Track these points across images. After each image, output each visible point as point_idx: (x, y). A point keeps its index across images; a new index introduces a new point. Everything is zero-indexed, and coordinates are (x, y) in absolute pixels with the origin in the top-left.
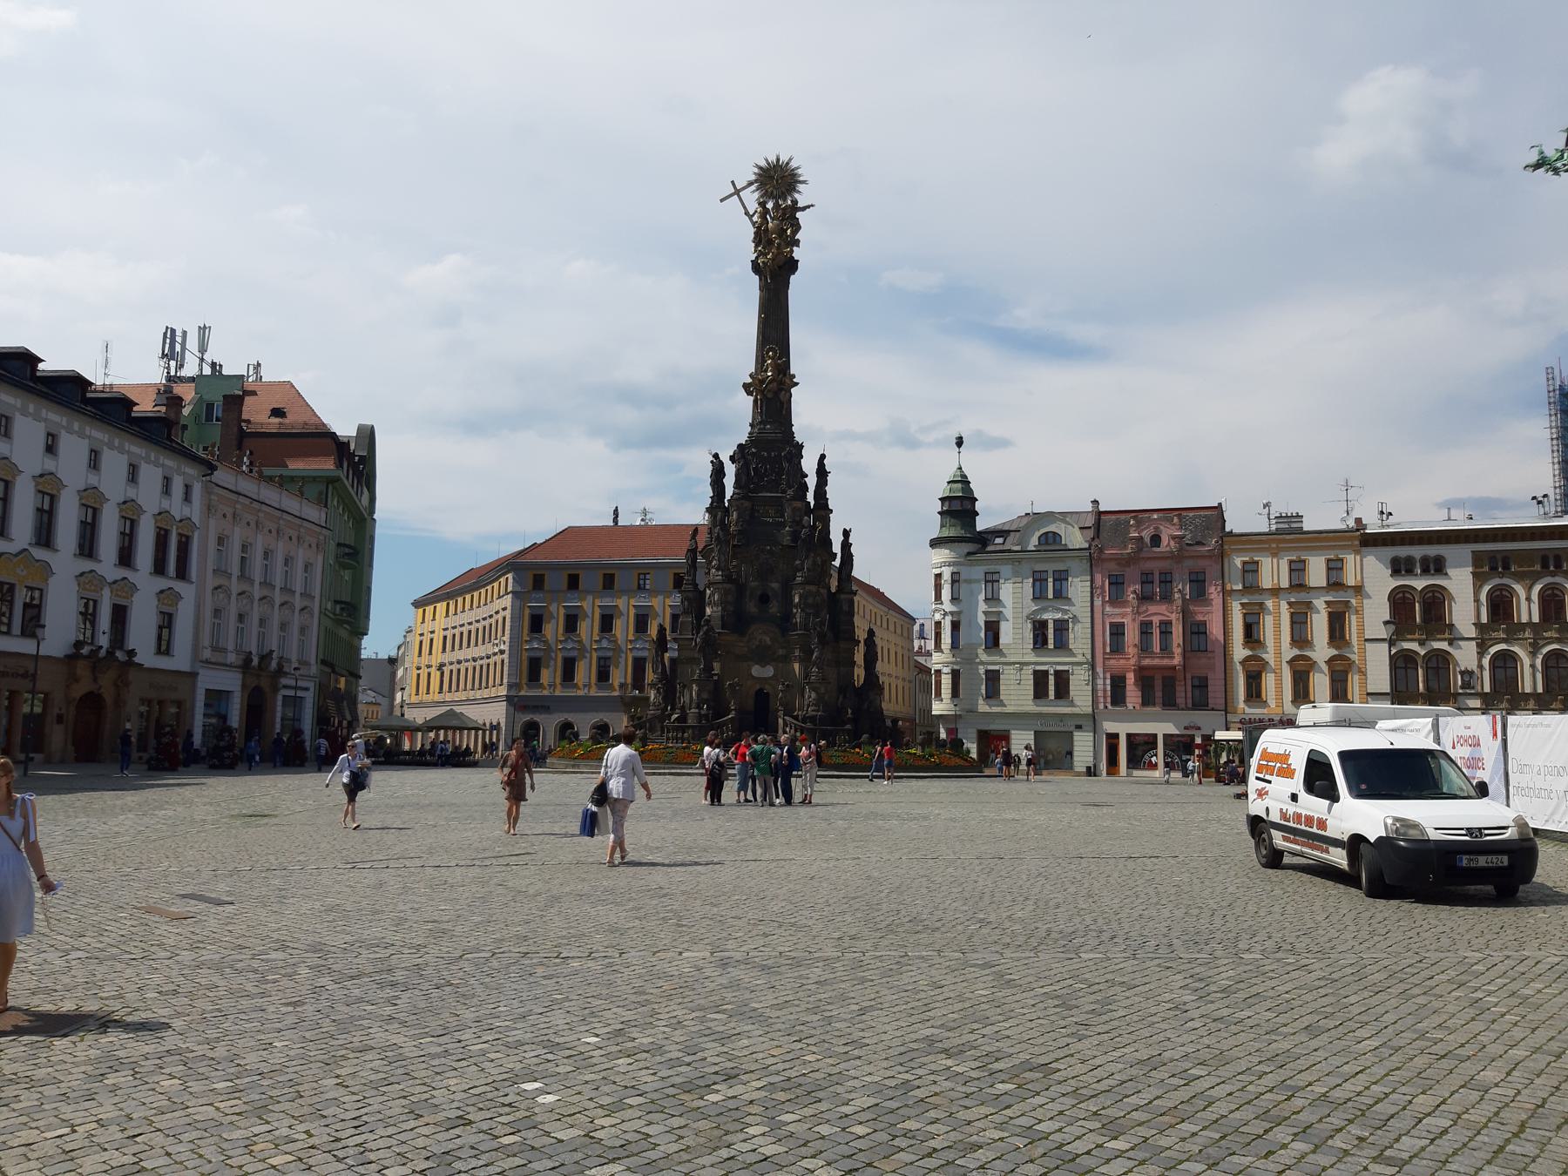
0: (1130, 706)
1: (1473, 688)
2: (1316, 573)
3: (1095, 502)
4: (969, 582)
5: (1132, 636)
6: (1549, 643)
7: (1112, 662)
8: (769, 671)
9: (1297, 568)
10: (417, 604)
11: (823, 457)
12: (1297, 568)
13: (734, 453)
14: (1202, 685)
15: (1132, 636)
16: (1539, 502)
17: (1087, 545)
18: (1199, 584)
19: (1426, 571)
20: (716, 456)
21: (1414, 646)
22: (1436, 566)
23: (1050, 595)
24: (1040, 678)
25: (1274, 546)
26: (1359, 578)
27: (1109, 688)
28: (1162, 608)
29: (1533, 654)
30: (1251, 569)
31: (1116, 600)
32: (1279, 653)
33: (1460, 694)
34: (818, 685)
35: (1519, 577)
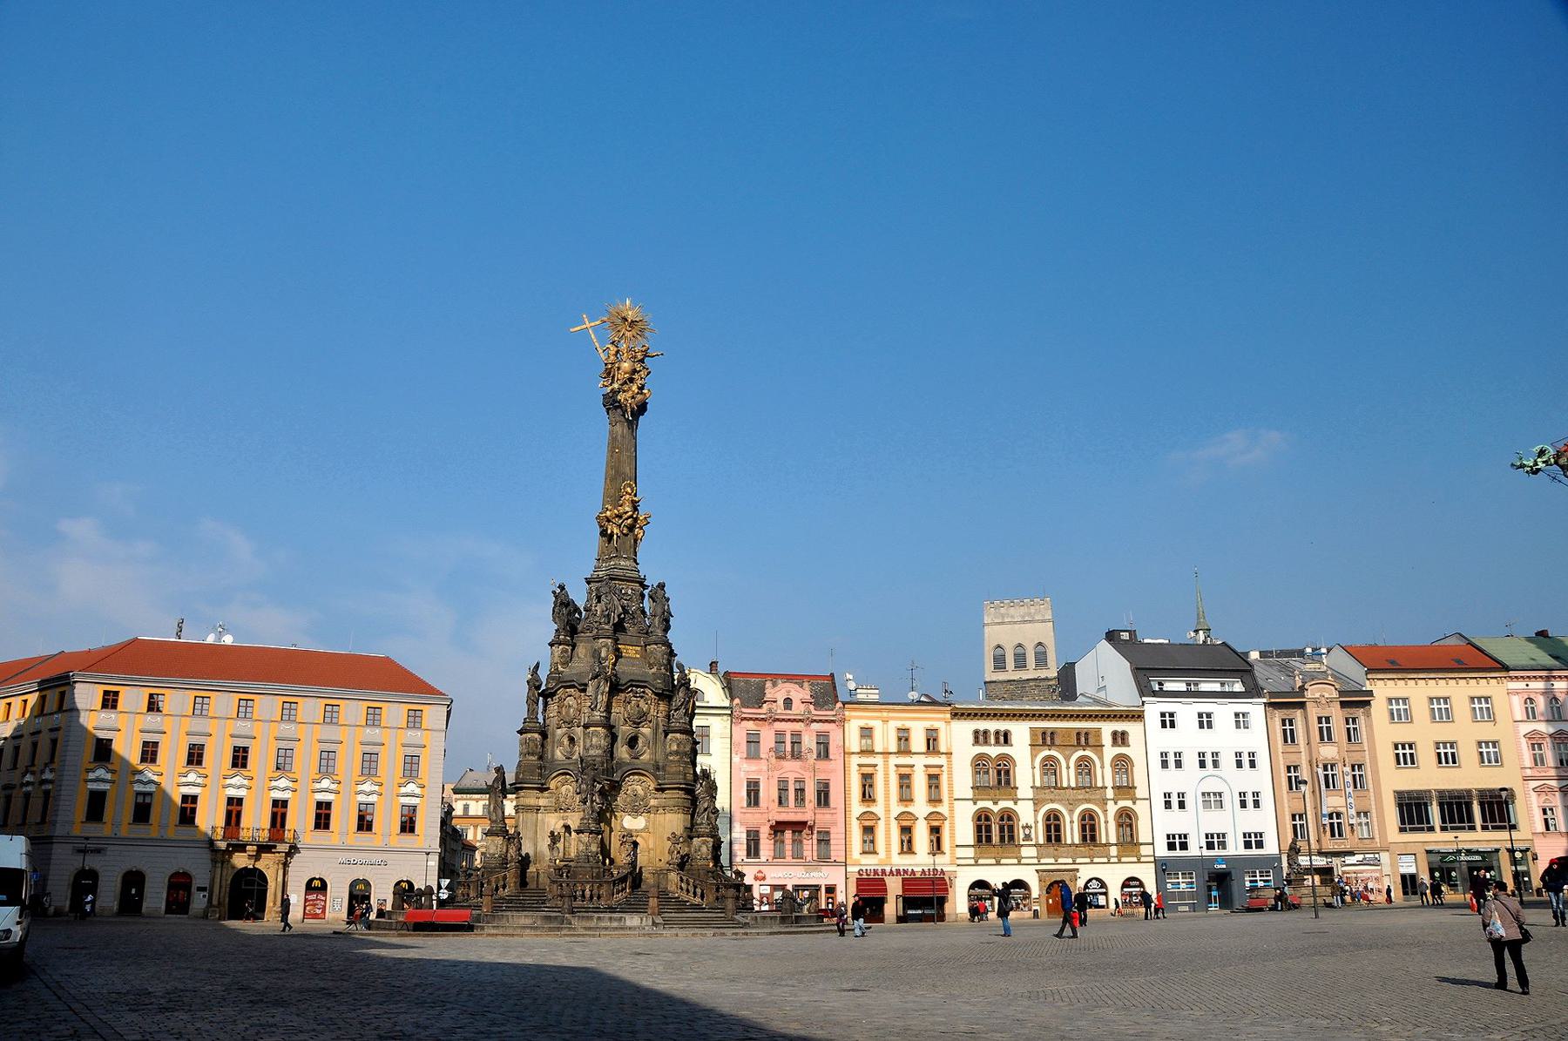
0: (763, 859)
2: (918, 742)
9: (904, 737)
12: (904, 737)
14: (824, 840)
15: (768, 793)
17: (727, 703)
19: (997, 742)
20: (562, 588)
21: (989, 804)
22: (1005, 738)
25: (885, 714)
28: (796, 764)
29: (1071, 812)
30: (867, 732)
32: (888, 811)
33: (1022, 846)
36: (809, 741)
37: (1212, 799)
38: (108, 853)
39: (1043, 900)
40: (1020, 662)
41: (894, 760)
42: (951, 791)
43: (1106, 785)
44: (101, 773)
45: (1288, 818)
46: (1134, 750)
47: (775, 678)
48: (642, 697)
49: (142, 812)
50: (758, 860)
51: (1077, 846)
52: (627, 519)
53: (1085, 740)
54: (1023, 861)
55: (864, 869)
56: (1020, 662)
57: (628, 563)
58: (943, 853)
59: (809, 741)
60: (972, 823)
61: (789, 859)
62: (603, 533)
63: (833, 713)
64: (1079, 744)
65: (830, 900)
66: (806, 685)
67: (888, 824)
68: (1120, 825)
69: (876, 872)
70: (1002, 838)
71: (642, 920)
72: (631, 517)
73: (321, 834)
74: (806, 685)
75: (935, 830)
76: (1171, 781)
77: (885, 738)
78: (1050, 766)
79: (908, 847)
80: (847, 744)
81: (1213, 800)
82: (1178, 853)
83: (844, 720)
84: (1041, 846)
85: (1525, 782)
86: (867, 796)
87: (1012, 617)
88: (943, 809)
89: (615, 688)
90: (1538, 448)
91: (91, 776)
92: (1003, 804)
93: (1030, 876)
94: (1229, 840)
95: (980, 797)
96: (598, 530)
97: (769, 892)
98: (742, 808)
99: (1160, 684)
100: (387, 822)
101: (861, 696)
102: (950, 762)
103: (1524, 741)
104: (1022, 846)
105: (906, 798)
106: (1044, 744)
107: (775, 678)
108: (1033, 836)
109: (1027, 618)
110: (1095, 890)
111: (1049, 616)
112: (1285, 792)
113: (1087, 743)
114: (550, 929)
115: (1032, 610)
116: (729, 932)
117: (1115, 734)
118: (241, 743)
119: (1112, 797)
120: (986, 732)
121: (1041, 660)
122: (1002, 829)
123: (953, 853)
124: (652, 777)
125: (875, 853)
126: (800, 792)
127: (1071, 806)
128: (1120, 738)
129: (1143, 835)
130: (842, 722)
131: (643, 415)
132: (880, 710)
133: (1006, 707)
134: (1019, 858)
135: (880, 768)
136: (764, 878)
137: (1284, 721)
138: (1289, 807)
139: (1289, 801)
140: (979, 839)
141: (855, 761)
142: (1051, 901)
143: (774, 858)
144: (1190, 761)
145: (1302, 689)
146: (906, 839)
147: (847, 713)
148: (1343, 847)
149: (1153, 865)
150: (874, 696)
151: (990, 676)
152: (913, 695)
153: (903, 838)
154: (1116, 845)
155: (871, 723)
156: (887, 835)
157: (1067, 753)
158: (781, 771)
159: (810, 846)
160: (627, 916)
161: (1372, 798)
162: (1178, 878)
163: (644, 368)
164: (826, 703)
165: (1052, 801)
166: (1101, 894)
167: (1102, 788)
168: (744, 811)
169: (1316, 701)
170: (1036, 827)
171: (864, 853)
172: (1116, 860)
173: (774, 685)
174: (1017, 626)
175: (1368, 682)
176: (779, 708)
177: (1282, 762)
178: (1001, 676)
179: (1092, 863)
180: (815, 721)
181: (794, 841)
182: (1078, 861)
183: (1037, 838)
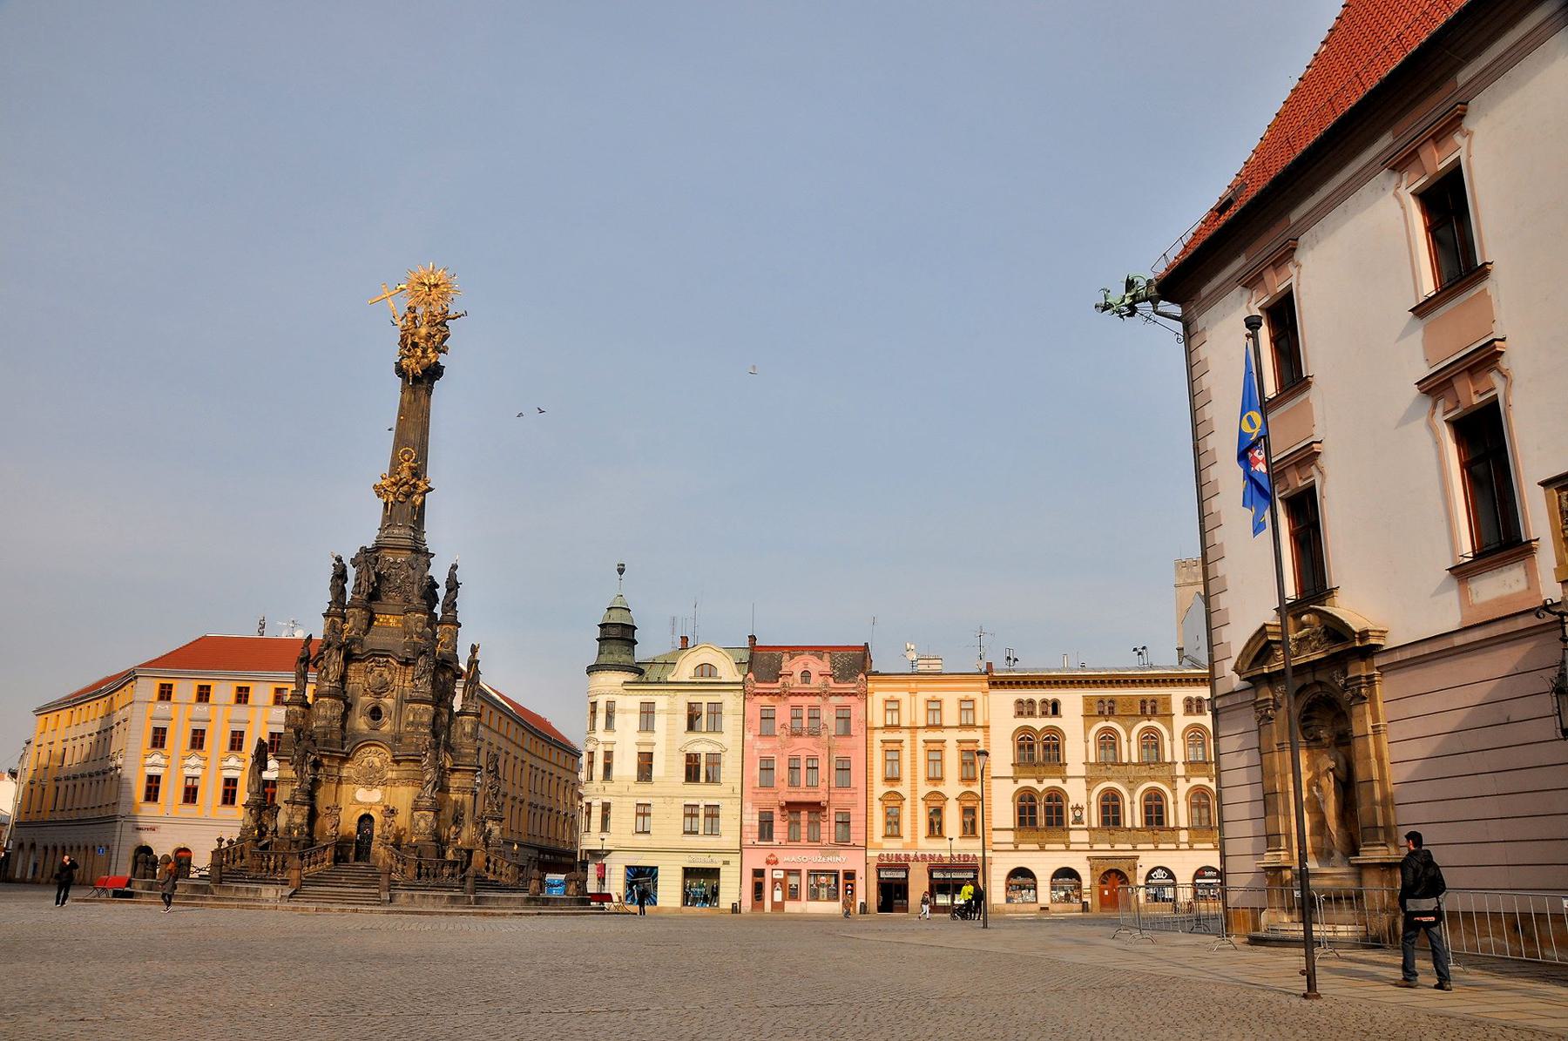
0: (776, 842)
1: (1083, 823)
2: (951, 715)
3: (753, 638)
4: (624, 712)
5: (781, 770)
6: (1146, 782)
7: (761, 796)
8: (375, 795)
9: (935, 706)
10: (41, 711)
11: (455, 567)
12: (935, 706)
13: (356, 557)
15: (781, 770)
16: (1140, 654)
17: (740, 678)
18: (844, 719)
19: (1044, 714)
20: (339, 559)
21: (1032, 783)
22: (1055, 708)
23: (704, 729)
24: (691, 812)
25: (913, 685)
26: (986, 718)
27: (757, 823)
29: (1132, 791)
30: (892, 705)
31: (765, 734)
32: (914, 791)
33: (1071, 829)
34: (426, 812)
36: (828, 716)
38: (161, 831)
39: (1096, 891)
41: (922, 735)
44: (157, 758)
47: (795, 651)
48: (385, 666)
49: (190, 795)
50: (770, 843)
51: (1138, 830)
52: (401, 486)
53: (1152, 708)
55: (885, 853)
57: (402, 531)
59: (828, 716)
61: (804, 842)
63: (854, 685)
64: (1143, 713)
65: (849, 887)
66: (826, 656)
67: (914, 805)
68: (1192, 806)
69: (898, 857)
70: (1049, 823)
71: (277, 892)
73: (189, 808)
74: (826, 656)
75: (968, 812)
78: (1108, 741)
79: (935, 828)
84: (1094, 829)
89: (349, 658)
91: (149, 761)
92: (1048, 783)
97: (782, 877)
98: (755, 788)
100: (211, 792)
102: (987, 738)
104: (1071, 829)
106: (1101, 713)
108: (1085, 818)
110: (1161, 881)
113: (1154, 712)
116: (336, 907)
117: (1189, 700)
118: (237, 728)
119: (1183, 774)
120: (1031, 702)
122: (1048, 810)
124: (388, 749)
125: (899, 836)
127: (1132, 784)
130: (865, 695)
135: (907, 744)
136: (776, 862)
140: (1022, 821)
142: (1106, 893)
146: (968, 820)
153: (966, 820)
155: (897, 695)
157: (1129, 723)
158: (790, 750)
160: (263, 887)
165: (1109, 779)
166: (1168, 885)
167: (1170, 763)
168: (758, 791)
170: (1089, 808)
171: (886, 836)
172: (1187, 846)
173: (791, 658)
179: (1156, 849)
180: (833, 694)
181: (810, 822)
183: (1089, 821)
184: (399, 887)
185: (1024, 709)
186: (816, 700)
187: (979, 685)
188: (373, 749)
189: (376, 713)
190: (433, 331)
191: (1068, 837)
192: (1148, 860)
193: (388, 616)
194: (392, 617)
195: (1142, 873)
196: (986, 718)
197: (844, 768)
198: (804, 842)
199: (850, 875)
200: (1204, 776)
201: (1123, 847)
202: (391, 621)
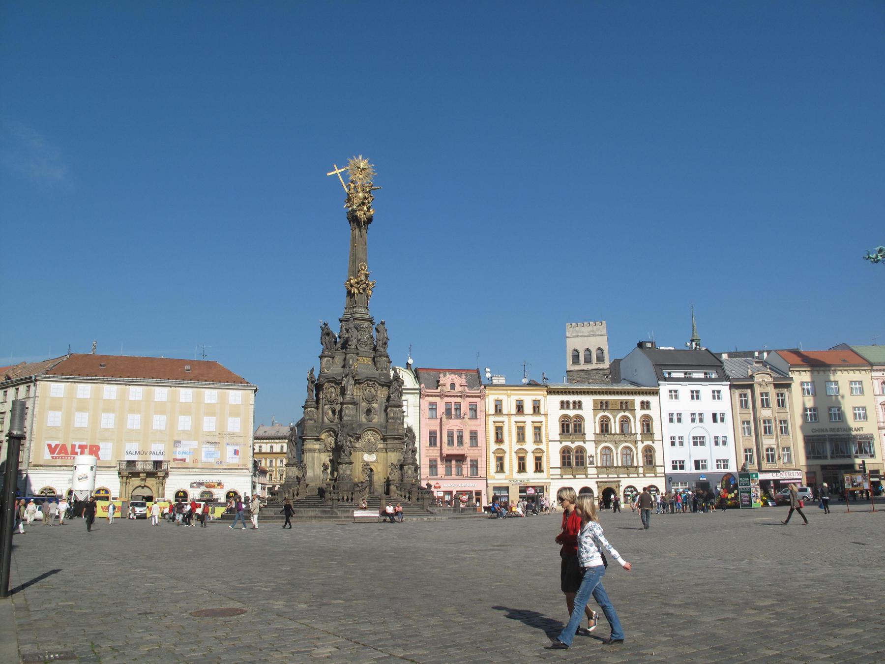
0: (439, 476)
1: (594, 464)
2: (528, 408)
14: (474, 465)
17: (417, 386)
18: (474, 409)
21: (569, 444)
22: (578, 405)
25: (509, 392)
26: (546, 410)
29: (617, 448)
32: (511, 448)
35: (612, 410)
37: (698, 440)
40: (588, 359)
42: (547, 436)
43: (637, 432)
45: (742, 451)
46: (653, 412)
48: (372, 387)
52: (362, 284)
53: (626, 406)
54: (589, 476)
56: (588, 359)
58: (542, 471)
60: (559, 455)
61: (454, 476)
62: (350, 294)
63: (479, 391)
66: (463, 376)
67: (511, 455)
70: (577, 464)
72: (365, 283)
74: (463, 376)
75: (538, 460)
76: (675, 430)
77: (509, 406)
79: (522, 468)
80: (487, 410)
81: (698, 441)
82: (678, 471)
83: (484, 396)
84: (599, 467)
85: (880, 430)
86: (499, 440)
87: (583, 332)
88: (543, 446)
90: (878, 248)
92: (577, 444)
93: (592, 484)
94: (709, 464)
95: (564, 440)
96: (346, 291)
97: (442, 495)
99: (669, 373)
101: (495, 381)
103: (880, 406)
105: (521, 438)
106: (601, 409)
107: (445, 371)
109: (592, 333)
111: (605, 332)
112: (741, 436)
114: (326, 518)
115: (595, 328)
117: (642, 403)
119: (640, 439)
120: (568, 402)
121: (601, 358)
122: (577, 458)
123: (548, 472)
126: (460, 438)
127: (616, 443)
128: (645, 405)
129: (658, 461)
131: (370, 224)
132: (506, 390)
133: (579, 387)
134: (586, 475)
135: (506, 423)
136: (440, 487)
137: (741, 396)
138: (743, 445)
139: (743, 441)
141: (491, 419)
143: (446, 475)
144: (686, 418)
145: (752, 377)
147: (487, 392)
148: (774, 468)
149: (664, 478)
150: (502, 381)
151: (570, 366)
152: (525, 381)
154: (642, 467)
155: (500, 397)
156: (510, 463)
157: (615, 414)
158: (448, 426)
159: (466, 468)
161: (792, 440)
162: (678, 486)
163: (370, 196)
164: (474, 386)
165: (605, 442)
167: (634, 434)
168: (428, 448)
169: (760, 384)
170: (596, 457)
173: (445, 375)
174: (586, 338)
175: (790, 373)
176: (448, 388)
177: (739, 419)
178: (577, 368)
179: (629, 477)
182: (621, 476)
183: (597, 463)
184: (412, 506)
185: (564, 405)
186: (459, 400)
187: (542, 393)
188: (370, 432)
189: (369, 411)
190: (367, 195)
191: (587, 471)
192: (625, 483)
193: (364, 358)
194: (366, 358)
195: (622, 489)
196: (546, 410)
197: (474, 436)
198: (454, 476)
199: (478, 493)
200: (650, 441)
201: (613, 476)
202: (365, 360)
